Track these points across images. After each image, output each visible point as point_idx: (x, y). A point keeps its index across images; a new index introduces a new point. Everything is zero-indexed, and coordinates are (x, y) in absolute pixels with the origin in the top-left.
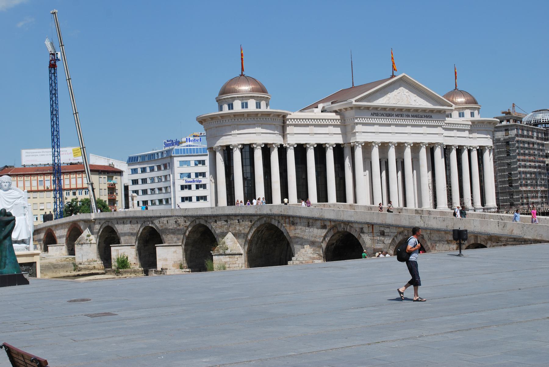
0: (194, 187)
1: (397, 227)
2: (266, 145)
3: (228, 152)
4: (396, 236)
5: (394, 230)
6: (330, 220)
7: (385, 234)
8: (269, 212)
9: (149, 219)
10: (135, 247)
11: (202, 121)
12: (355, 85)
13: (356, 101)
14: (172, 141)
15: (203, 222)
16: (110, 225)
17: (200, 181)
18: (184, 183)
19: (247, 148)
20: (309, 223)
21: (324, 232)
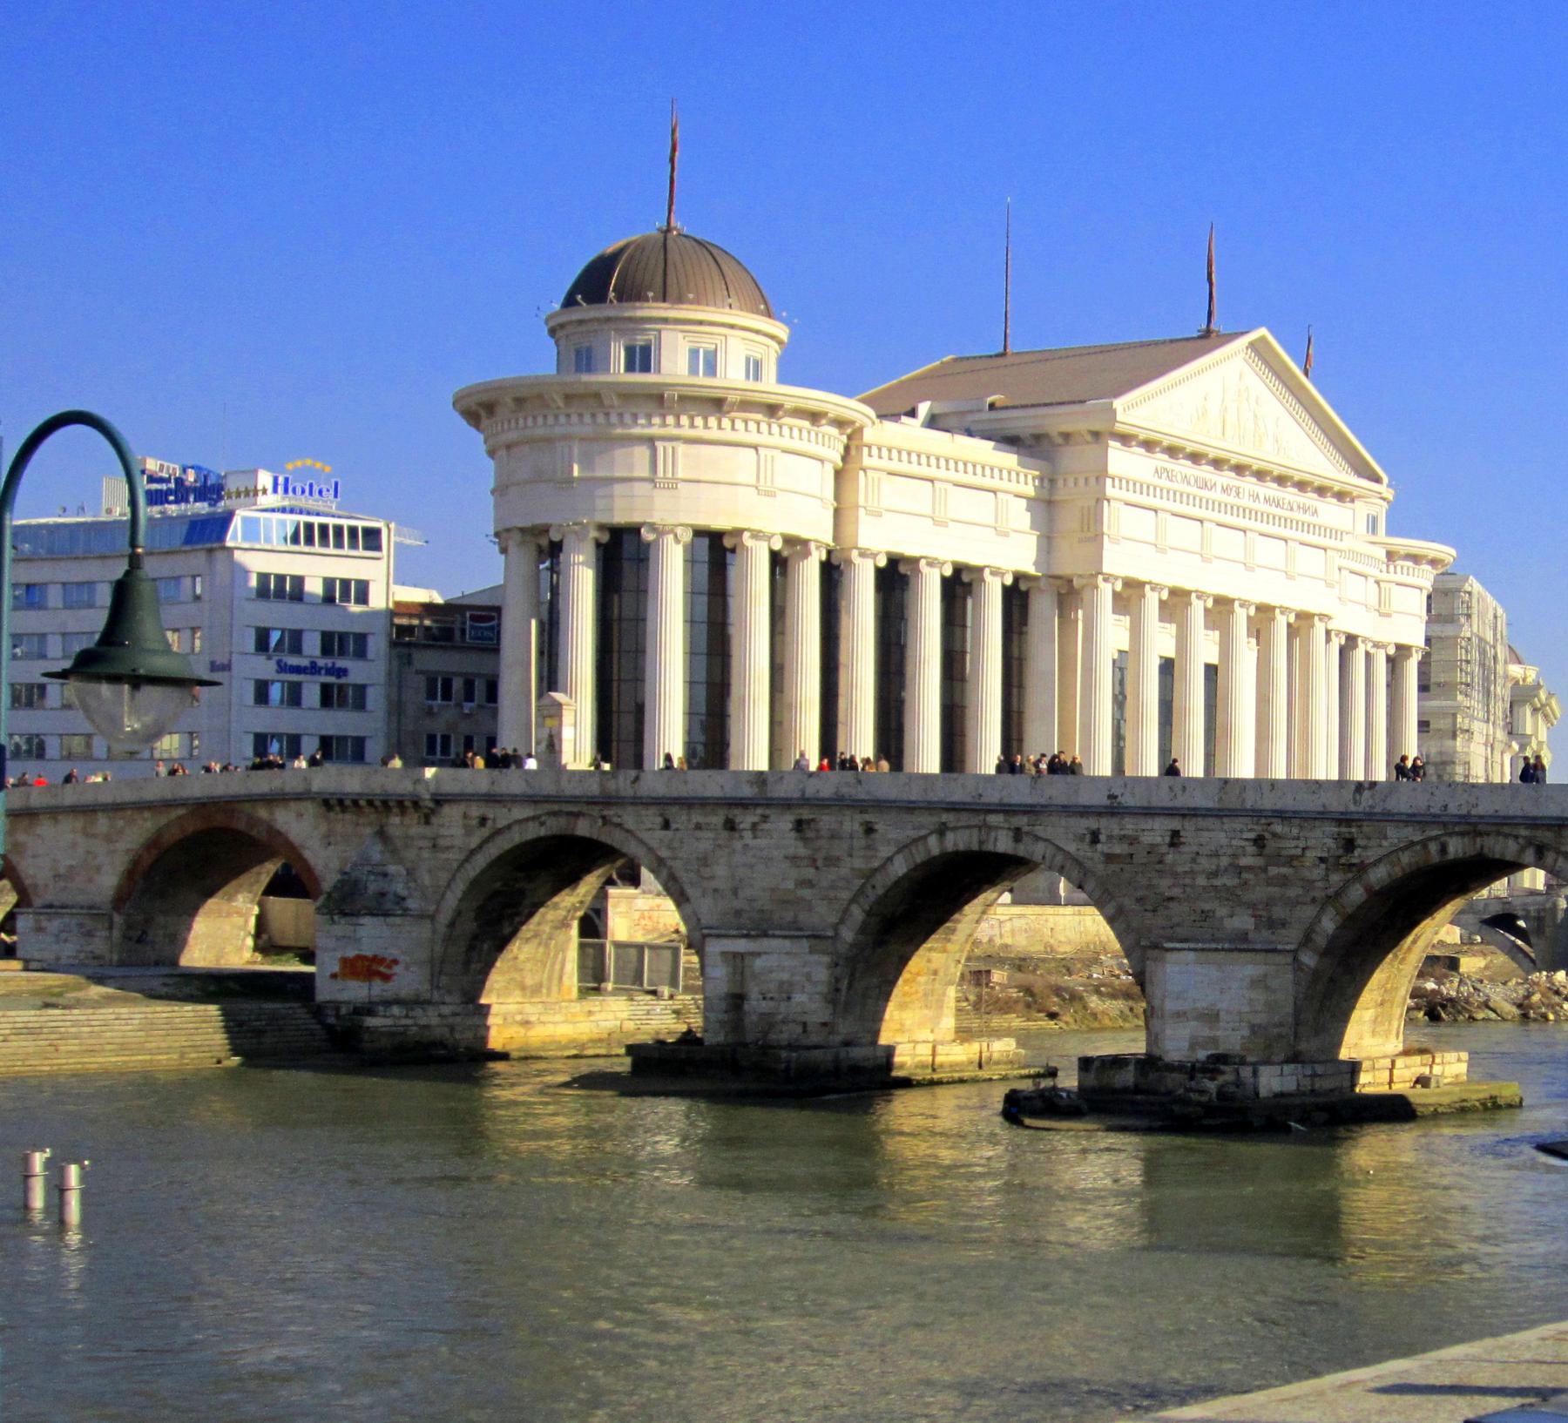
2: (789, 541)
3: (623, 556)
9: (994, 819)
17: (342, 672)
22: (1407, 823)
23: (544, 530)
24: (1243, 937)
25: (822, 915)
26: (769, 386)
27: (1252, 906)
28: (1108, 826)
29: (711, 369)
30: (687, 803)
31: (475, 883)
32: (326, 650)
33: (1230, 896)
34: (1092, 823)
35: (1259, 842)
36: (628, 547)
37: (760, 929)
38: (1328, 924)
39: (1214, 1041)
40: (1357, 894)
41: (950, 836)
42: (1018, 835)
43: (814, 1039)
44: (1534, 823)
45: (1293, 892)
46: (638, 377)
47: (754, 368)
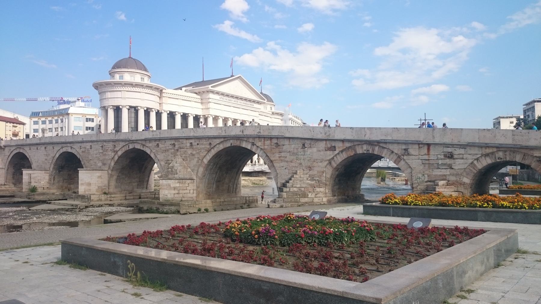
1: (481, 146)
2: (148, 109)
3: (118, 110)
4: (477, 159)
5: (477, 152)
6: (343, 141)
7: (455, 156)
8: (241, 133)
9: (68, 145)
10: (48, 172)
13: (212, 87)
15: (138, 146)
16: (21, 151)
19: (133, 110)
20: (304, 145)
21: (330, 154)
24: (100, 167)
25: (47, 166)
31: (10, 162)
34: (80, 144)
38: (113, 164)
39: (90, 189)
40: (116, 158)
42: (71, 148)
45: (107, 157)
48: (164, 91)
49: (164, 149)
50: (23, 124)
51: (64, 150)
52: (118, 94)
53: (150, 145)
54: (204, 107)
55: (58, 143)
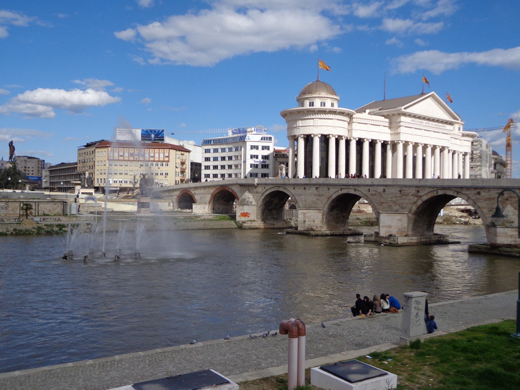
0: (260, 166)
2: (339, 136)
3: (309, 139)
9: (350, 187)
11: (284, 115)
12: (386, 98)
14: (240, 130)
18: (253, 163)
19: (323, 137)
22: (430, 187)
23: (295, 136)
24: (397, 211)
26: (336, 107)
27: (399, 204)
28: (372, 189)
29: (324, 105)
30: (320, 185)
31: (264, 199)
32: (263, 158)
33: (395, 203)
34: (368, 188)
35: (400, 191)
36: (310, 138)
37: (309, 208)
38: (414, 208)
39: (390, 231)
40: (420, 202)
41: (343, 190)
42: (355, 190)
43: (319, 229)
44: (456, 187)
46: (311, 107)
47: (332, 105)
48: (354, 116)
49: (488, 197)
50: (189, 151)
51: (345, 191)
52: (311, 122)
53: (468, 192)
54: (393, 132)
55: (336, 185)
